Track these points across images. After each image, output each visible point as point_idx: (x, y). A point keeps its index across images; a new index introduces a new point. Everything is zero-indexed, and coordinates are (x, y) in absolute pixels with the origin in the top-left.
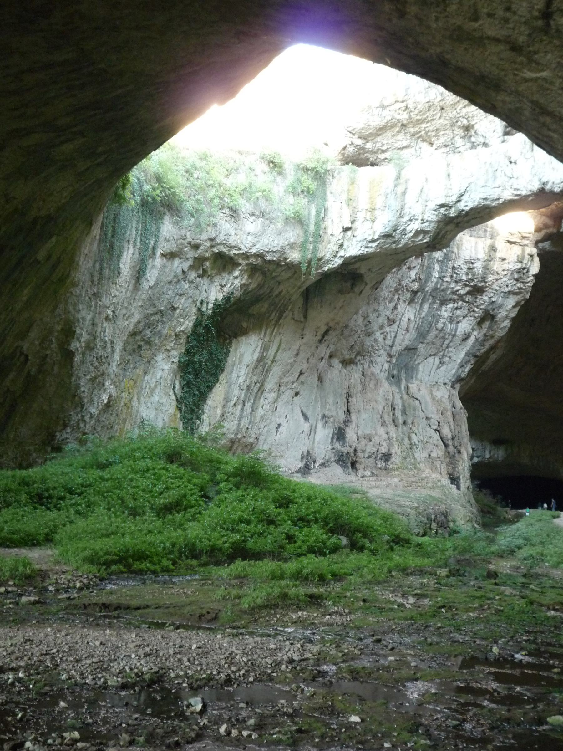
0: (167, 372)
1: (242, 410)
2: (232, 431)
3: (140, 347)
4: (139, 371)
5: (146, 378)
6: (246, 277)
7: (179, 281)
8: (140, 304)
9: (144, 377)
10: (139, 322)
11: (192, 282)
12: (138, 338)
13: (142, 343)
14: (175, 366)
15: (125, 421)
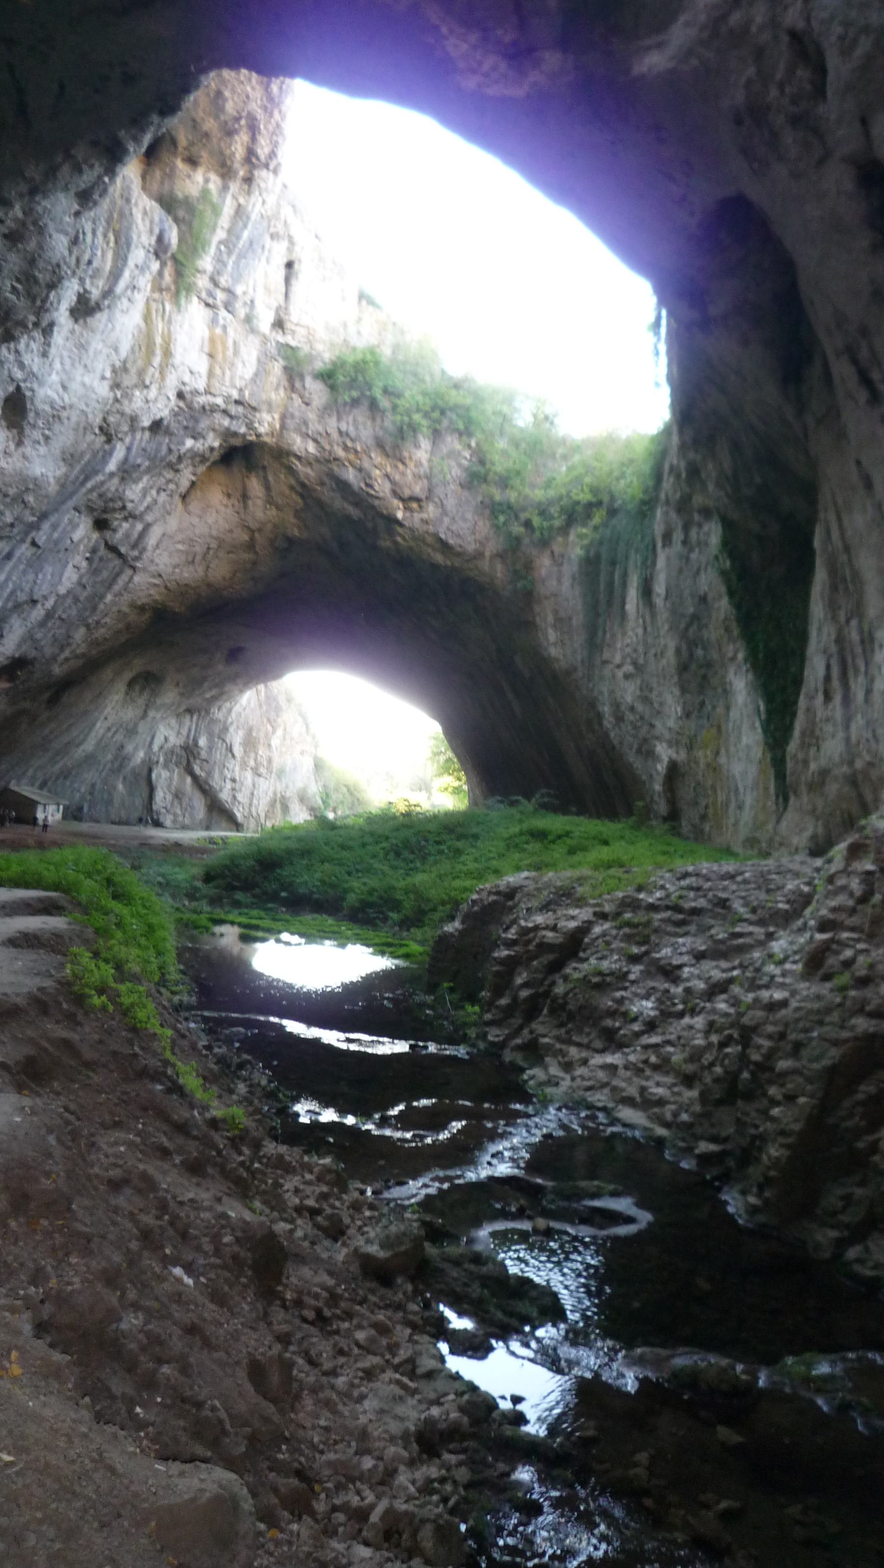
0: (744, 692)
1: (847, 700)
2: (837, 759)
3: (704, 677)
4: (720, 710)
5: (731, 714)
6: (710, 466)
7: (688, 559)
8: (666, 627)
9: (728, 715)
10: (678, 651)
11: (699, 543)
12: (693, 666)
13: (703, 671)
14: (750, 676)
15: (714, 788)
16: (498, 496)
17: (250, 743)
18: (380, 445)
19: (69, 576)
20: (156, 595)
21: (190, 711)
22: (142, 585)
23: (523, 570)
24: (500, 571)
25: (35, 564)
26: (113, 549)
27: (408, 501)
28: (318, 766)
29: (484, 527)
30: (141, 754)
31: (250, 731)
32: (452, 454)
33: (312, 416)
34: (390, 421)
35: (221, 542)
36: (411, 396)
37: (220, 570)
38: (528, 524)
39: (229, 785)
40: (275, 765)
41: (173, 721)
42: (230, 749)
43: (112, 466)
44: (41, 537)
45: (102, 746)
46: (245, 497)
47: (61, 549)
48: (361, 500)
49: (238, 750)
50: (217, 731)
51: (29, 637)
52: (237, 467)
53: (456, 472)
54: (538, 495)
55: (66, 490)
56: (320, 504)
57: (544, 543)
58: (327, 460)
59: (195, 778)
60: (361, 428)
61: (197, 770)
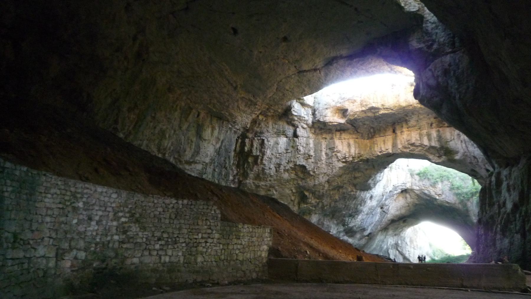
16: (456, 192)
17: (411, 241)
18: (431, 186)
19: (377, 218)
20: (392, 218)
21: (395, 235)
22: (389, 216)
23: (465, 205)
24: (460, 206)
25: (372, 217)
26: (384, 211)
27: (438, 195)
28: (430, 245)
29: (455, 198)
30: (385, 247)
31: (411, 238)
32: (446, 185)
33: (417, 182)
34: (433, 181)
35: (403, 207)
36: (436, 176)
37: (403, 211)
38: (464, 197)
39: (408, 252)
40: (419, 246)
41: (392, 238)
42: (406, 243)
43: (384, 199)
44: (373, 213)
45: (377, 246)
46: (406, 198)
47: (376, 214)
48: (429, 196)
49: (409, 243)
50: (402, 239)
51: (372, 229)
52: (404, 193)
53: (448, 188)
54: (465, 190)
55: (377, 205)
56: (420, 197)
57: (468, 200)
58: (421, 190)
59: (399, 251)
60: (427, 183)
61: (399, 249)
